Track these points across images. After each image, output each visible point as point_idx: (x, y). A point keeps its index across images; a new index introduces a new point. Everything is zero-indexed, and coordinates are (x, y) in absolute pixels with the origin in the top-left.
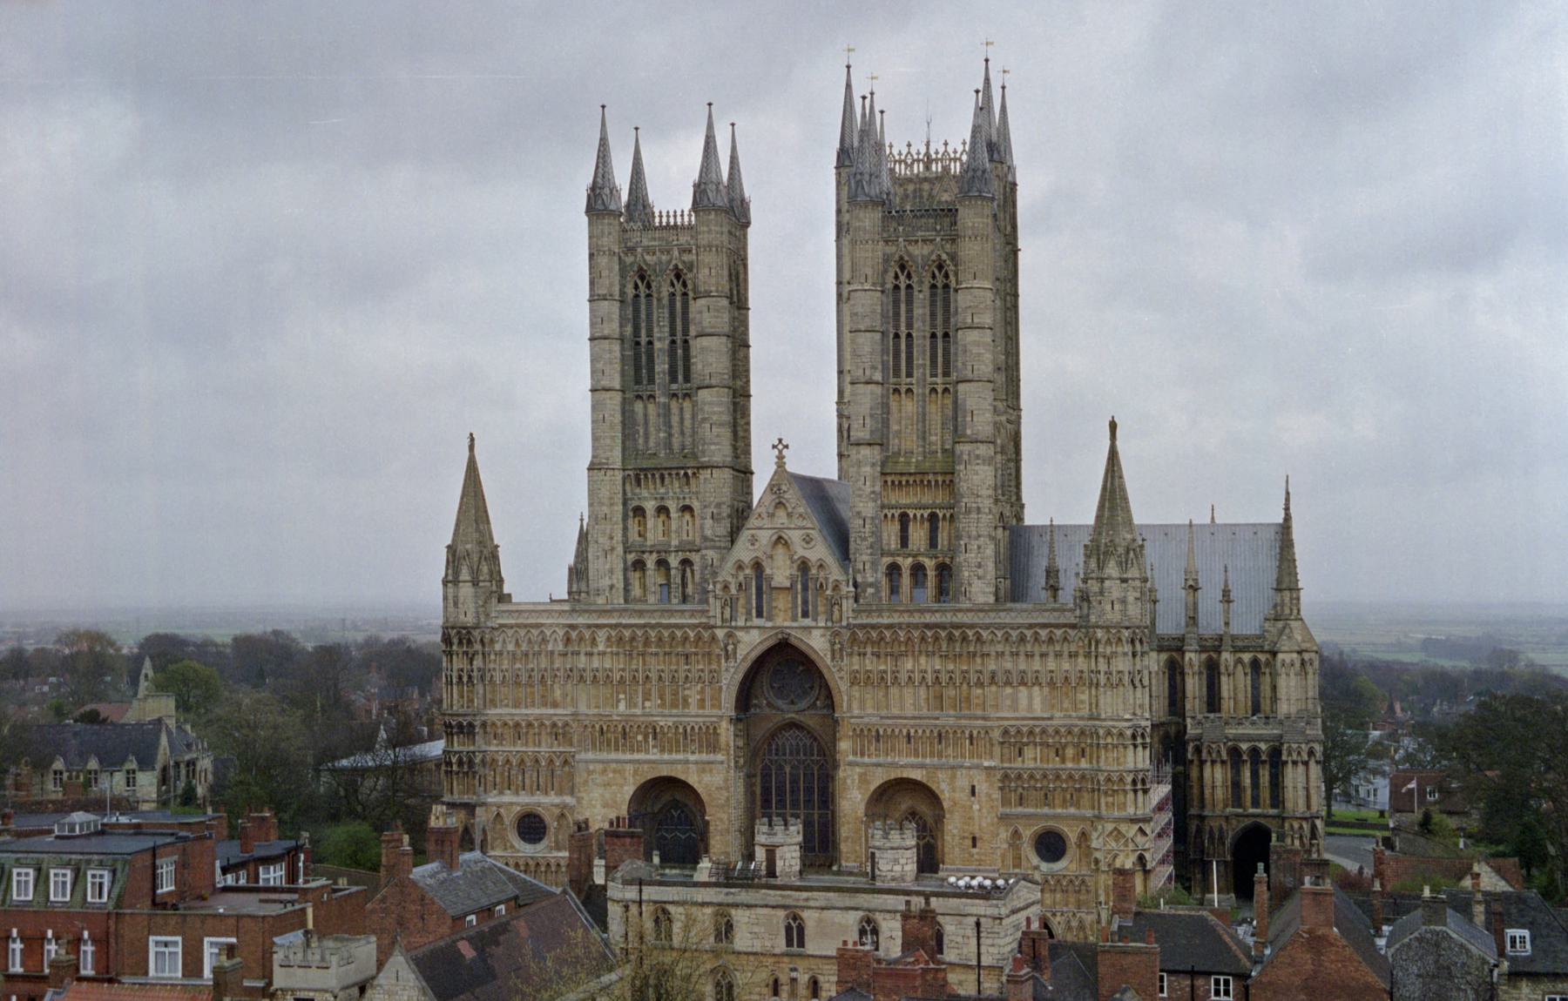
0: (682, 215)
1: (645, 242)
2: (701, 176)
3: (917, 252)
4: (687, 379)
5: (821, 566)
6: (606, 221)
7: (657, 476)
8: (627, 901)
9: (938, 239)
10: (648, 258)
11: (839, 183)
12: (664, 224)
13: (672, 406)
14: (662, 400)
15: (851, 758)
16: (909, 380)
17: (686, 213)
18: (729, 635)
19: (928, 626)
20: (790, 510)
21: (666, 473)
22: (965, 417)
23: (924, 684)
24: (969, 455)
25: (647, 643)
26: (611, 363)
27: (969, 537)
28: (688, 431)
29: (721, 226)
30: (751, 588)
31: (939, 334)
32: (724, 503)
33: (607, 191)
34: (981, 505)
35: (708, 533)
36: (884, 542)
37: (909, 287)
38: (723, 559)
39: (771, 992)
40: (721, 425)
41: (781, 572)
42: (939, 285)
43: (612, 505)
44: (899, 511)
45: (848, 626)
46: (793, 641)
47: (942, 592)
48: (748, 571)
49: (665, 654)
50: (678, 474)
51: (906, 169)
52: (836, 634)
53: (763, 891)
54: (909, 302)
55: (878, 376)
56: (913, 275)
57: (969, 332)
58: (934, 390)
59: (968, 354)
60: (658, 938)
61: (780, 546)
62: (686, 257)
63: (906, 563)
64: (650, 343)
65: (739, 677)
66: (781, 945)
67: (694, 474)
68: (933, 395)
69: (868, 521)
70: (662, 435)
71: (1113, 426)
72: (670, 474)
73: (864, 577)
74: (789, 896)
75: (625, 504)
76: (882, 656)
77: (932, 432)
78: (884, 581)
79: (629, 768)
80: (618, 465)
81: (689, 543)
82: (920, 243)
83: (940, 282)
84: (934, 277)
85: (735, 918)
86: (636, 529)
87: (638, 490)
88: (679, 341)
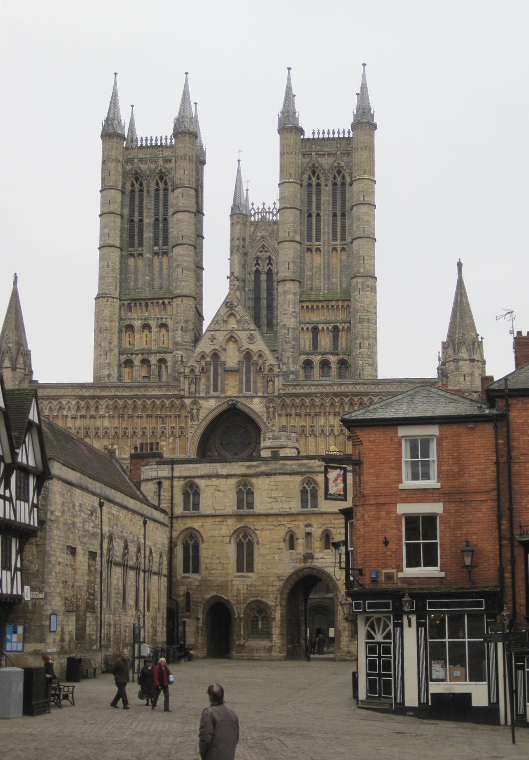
0: (166, 139)
1: (140, 155)
2: (180, 114)
3: (324, 162)
4: (166, 242)
6: (115, 140)
7: (143, 304)
8: (160, 478)
9: (339, 153)
10: (142, 166)
11: (232, 224)
12: (154, 144)
13: (154, 261)
14: (148, 255)
16: (317, 243)
17: (169, 138)
18: (194, 403)
19: (336, 395)
20: (238, 318)
21: (149, 302)
22: (359, 261)
23: (332, 434)
24: (362, 284)
25: (135, 408)
26: (114, 229)
27: (363, 338)
28: (165, 277)
29: (193, 145)
30: (210, 371)
31: (339, 214)
32: (190, 321)
33: (116, 122)
34: (370, 318)
35: (179, 339)
36: (301, 346)
37: (318, 185)
38: (189, 358)
39: (288, 546)
40: (188, 270)
41: (232, 358)
42: (339, 183)
43: (111, 321)
44: (312, 325)
45: (279, 396)
46: (239, 406)
47: (340, 376)
48: (208, 359)
49: (147, 417)
51: (273, 216)
52: (271, 401)
53: (281, 462)
54: (318, 194)
55: (298, 238)
56: (321, 176)
57: (360, 207)
58: (335, 249)
59: (361, 220)
60: (186, 508)
61: (231, 343)
62: (168, 166)
63: (317, 359)
64: (141, 221)
65: (200, 431)
66: (295, 505)
67: (169, 302)
68: (334, 253)
69: (291, 331)
70: (147, 278)
71: (460, 265)
72: (152, 303)
73: (288, 368)
74: (304, 465)
75: (121, 319)
76: (303, 415)
77: (334, 276)
78: (301, 372)
80: (117, 295)
81: (164, 348)
82: (326, 156)
83: (339, 180)
84: (335, 178)
85: (256, 486)
86: (127, 340)
87: (129, 314)
88: (161, 219)
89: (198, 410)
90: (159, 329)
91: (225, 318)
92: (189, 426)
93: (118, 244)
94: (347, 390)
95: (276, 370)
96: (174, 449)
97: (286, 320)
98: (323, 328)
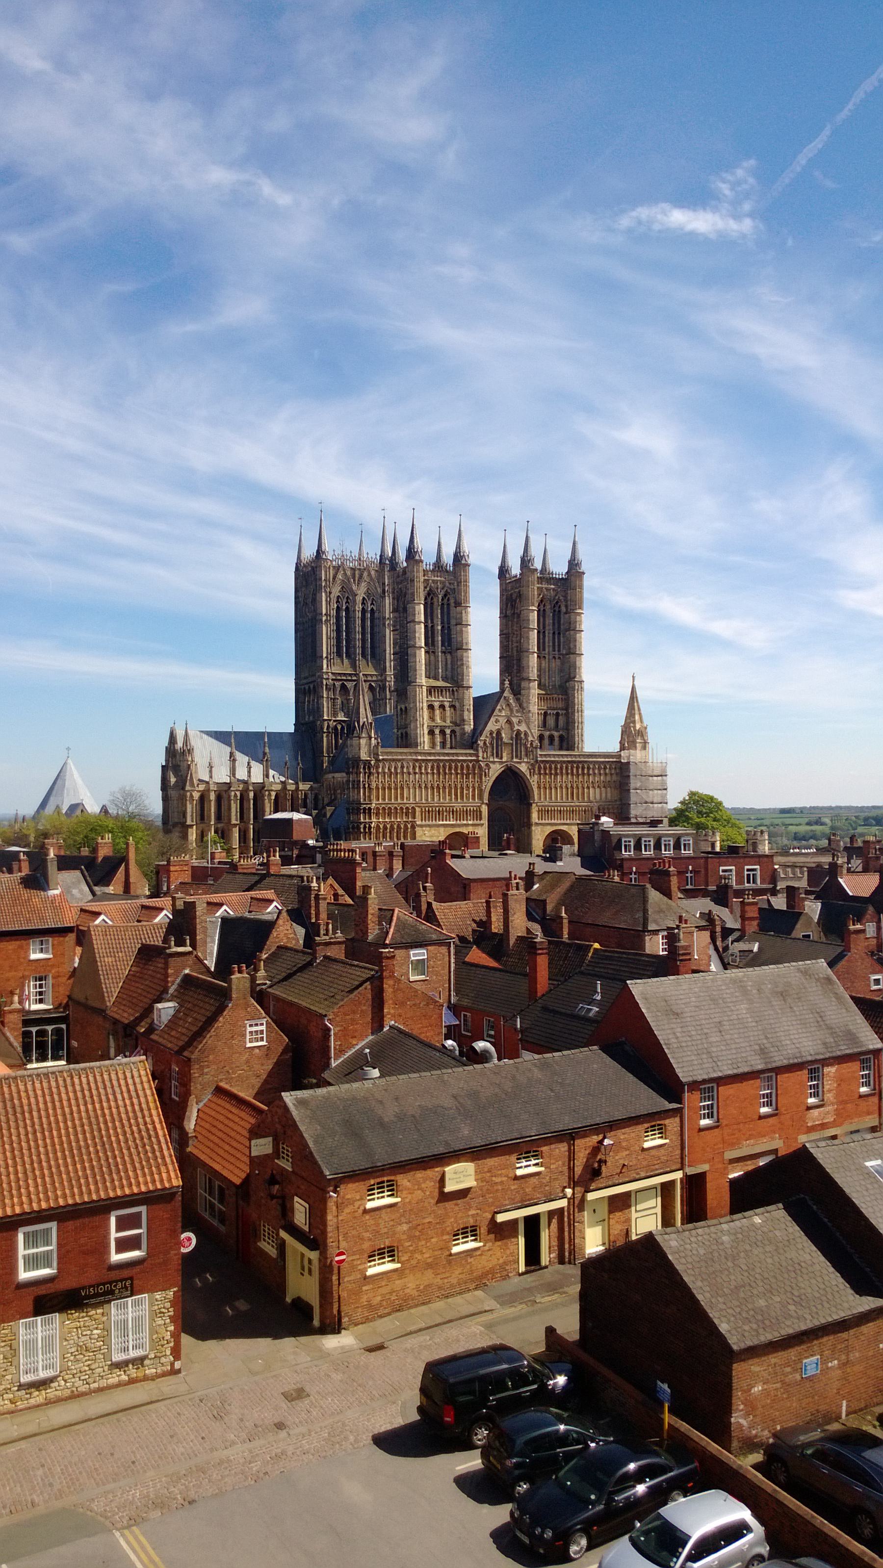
4: (450, 645)
15: (537, 821)
31: (556, 633)
37: (544, 610)
63: (547, 734)
65: (490, 784)
79: (442, 829)
93: (423, 645)
96: (473, 796)
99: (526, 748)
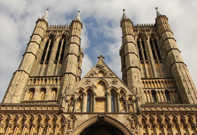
5: (122, 92)
44: (151, 90)
46: (107, 119)
48: (85, 91)
50: (53, 79)
61: (100, 86)
67: (60, 79)
72: (49, 79)
83: (153, 39)
89: (74, 122)
90: (50, 91)
91: (97, 72)
92: (65, 132)
94: (190, 110)
95: (134, 98)
97: (134, 84)
98: (158, 91)
99: (124, 103)
